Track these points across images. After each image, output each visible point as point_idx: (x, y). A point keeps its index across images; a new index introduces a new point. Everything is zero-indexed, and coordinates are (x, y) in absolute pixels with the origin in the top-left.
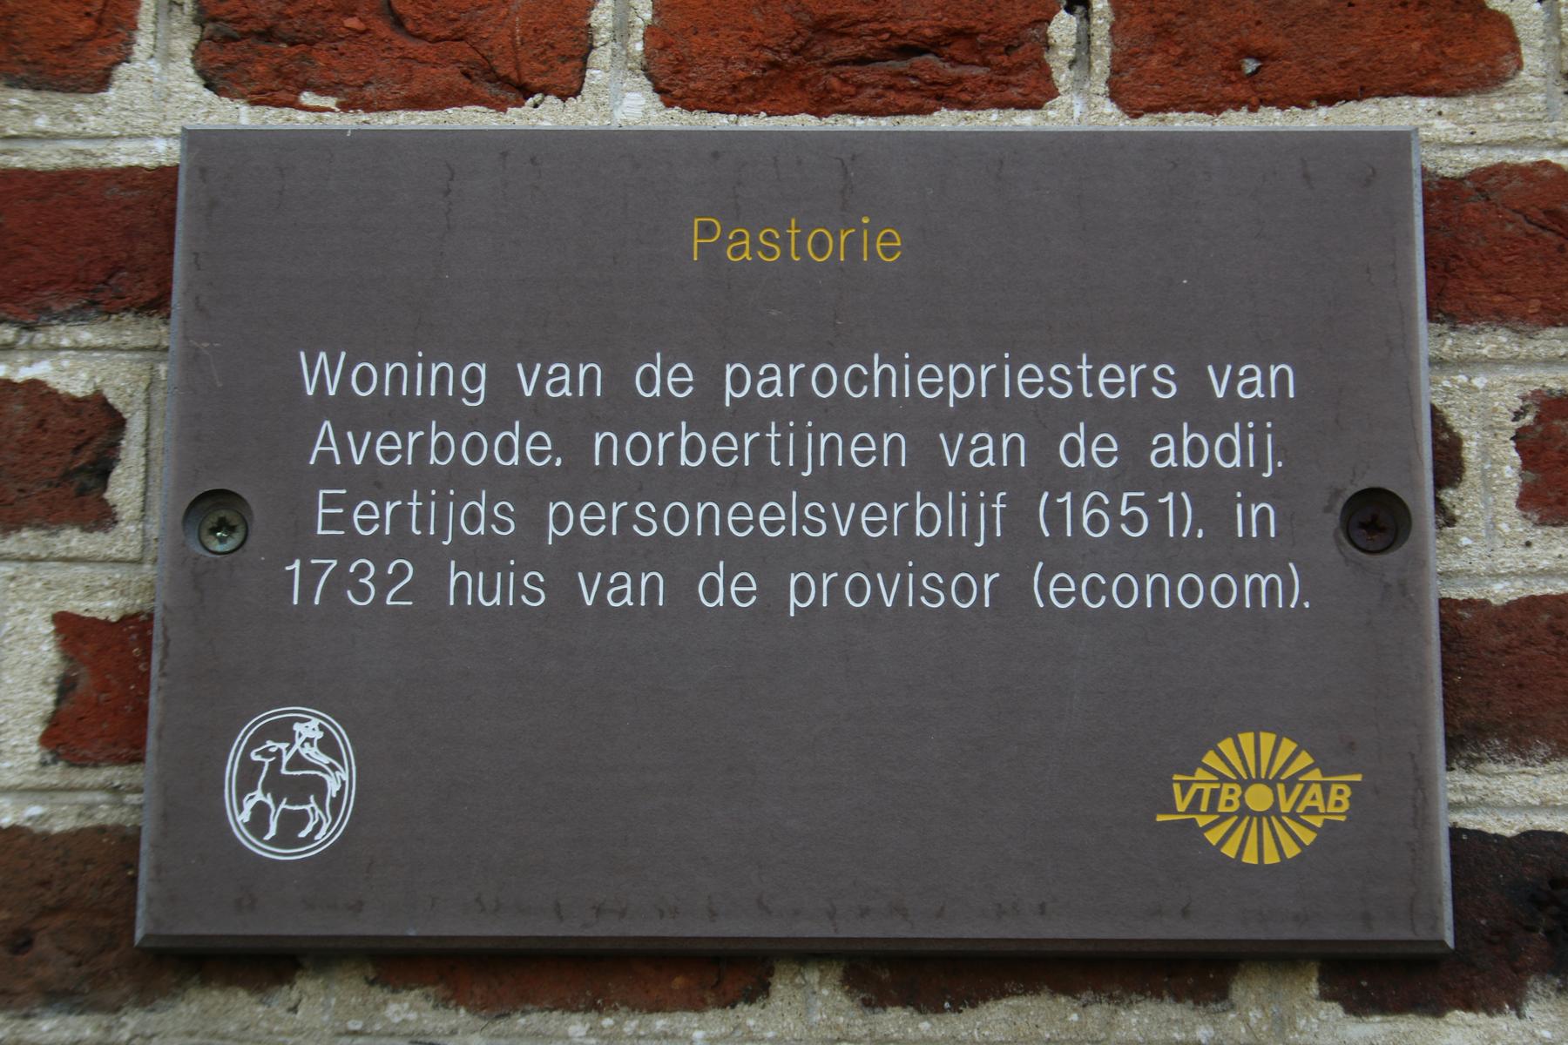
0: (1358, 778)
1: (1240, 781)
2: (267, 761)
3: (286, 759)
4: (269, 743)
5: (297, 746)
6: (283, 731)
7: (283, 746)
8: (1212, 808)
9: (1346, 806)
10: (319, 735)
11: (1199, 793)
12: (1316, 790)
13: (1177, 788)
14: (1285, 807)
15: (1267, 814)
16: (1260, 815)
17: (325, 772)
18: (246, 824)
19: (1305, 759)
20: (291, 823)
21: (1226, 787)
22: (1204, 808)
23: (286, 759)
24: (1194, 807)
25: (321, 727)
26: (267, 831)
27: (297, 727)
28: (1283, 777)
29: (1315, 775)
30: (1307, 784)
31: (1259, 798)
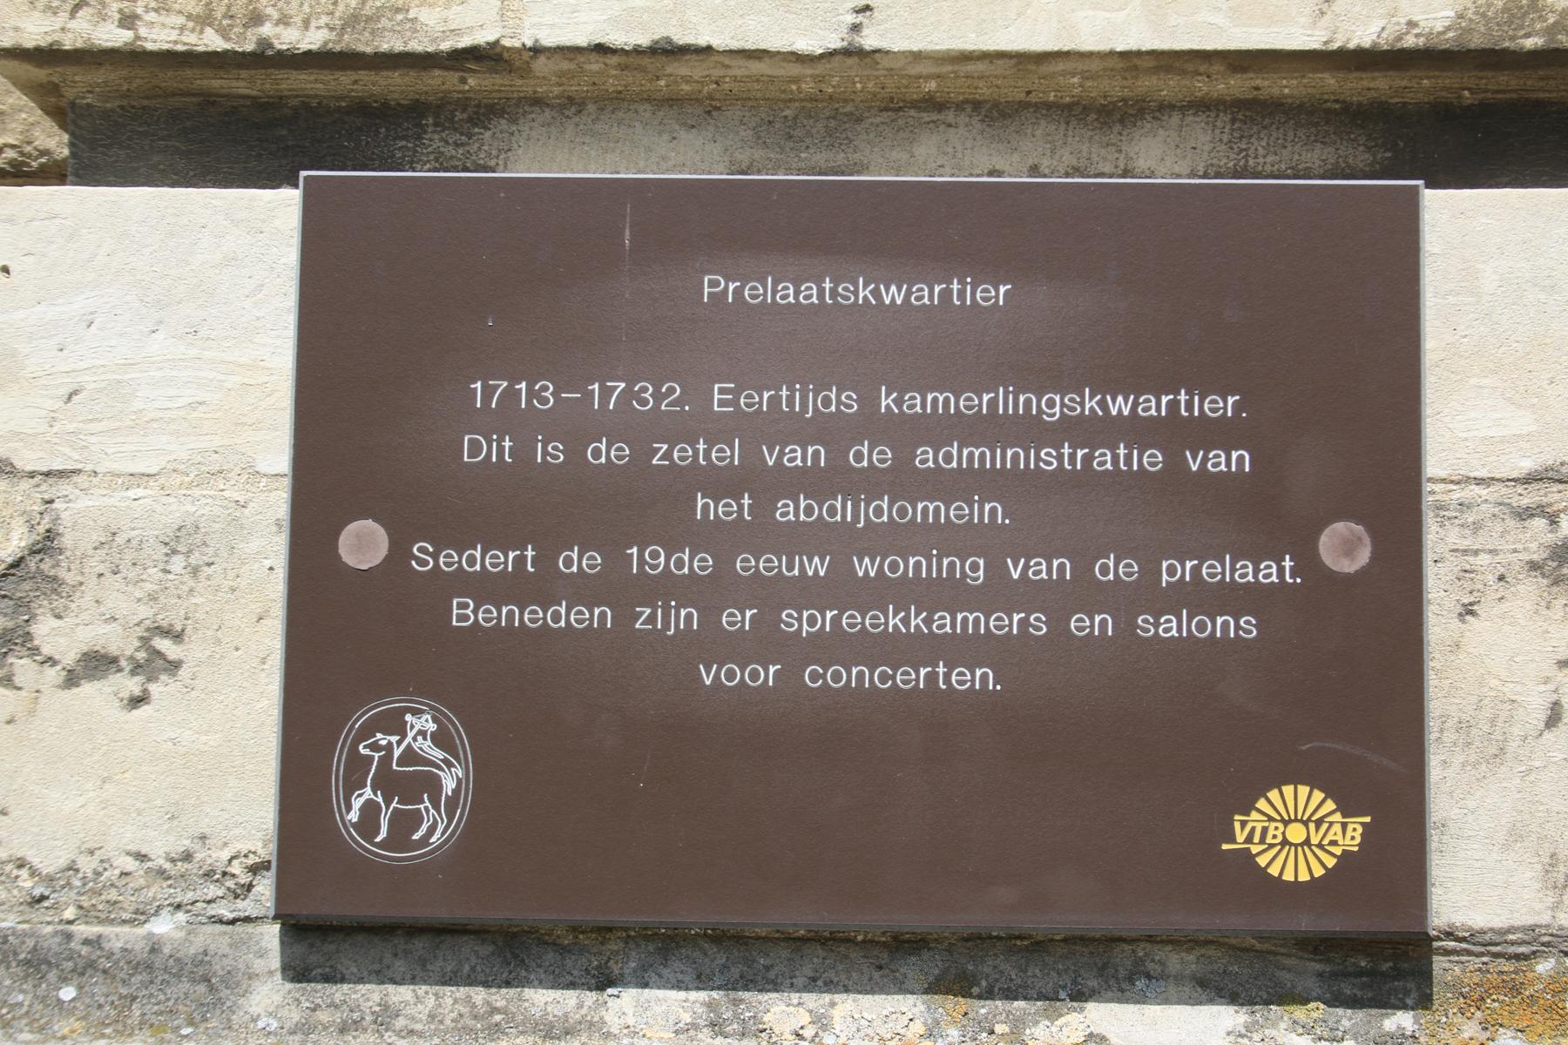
0: (1368, 819)
1: (1283, 820)
2: (377, 755)
3: (397, 753)
4: (379, 736)
5: (409, 739)
7: (394, 739)
9: (1358, 840)
11: (1253, 829)
12: (1337, 828)
13: (1237, 825)
14: (1315, 840)
15: (1302, 845)
18: (354, 825)
20: (405, 823)
21: (1273, 825)
22: (1256, 839)
23: (397, 753)
24: (1249, 840)
25: (435, 720)
27: (408, 717)
29: (1337, 817)
30: (1331, 824)
31: (1296, 833)
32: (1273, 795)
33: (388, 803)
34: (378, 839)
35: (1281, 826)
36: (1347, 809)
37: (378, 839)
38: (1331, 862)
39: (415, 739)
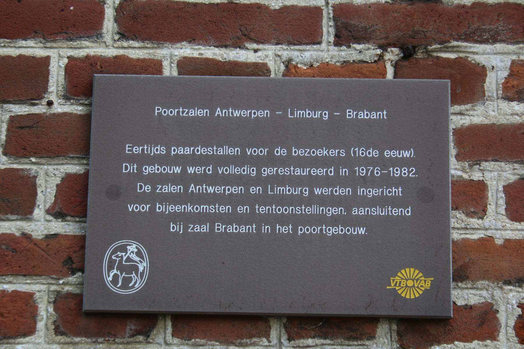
0: (432, 279)
2: (118, 259)
3: (125, 258)
4: (119, 253)
6: (123, 249)
8: (400, 285)
9: (429, 286)
10: (136, 250)
11: (397, 282)
12: (423, 282)
13: (392, 281)
14: (416, 286)
15: (412, 287)
16: (410, 287)
18: (111, 281)
19: (421, 275)
20: (127, 281)
21: (403, 281)
23: (125, 258)
24: (395, 285)
25: (137, 247)
26: (118, 284)
27: (128, 247)
29: (423, 278)
30: (421, 280)
31: (410, 283)
32: (403, 271)
33: (122, 274)
34: (118, 286)
36: (425, 276)
37: (118, 286)
38: (421, 292)
39: (130, 254)
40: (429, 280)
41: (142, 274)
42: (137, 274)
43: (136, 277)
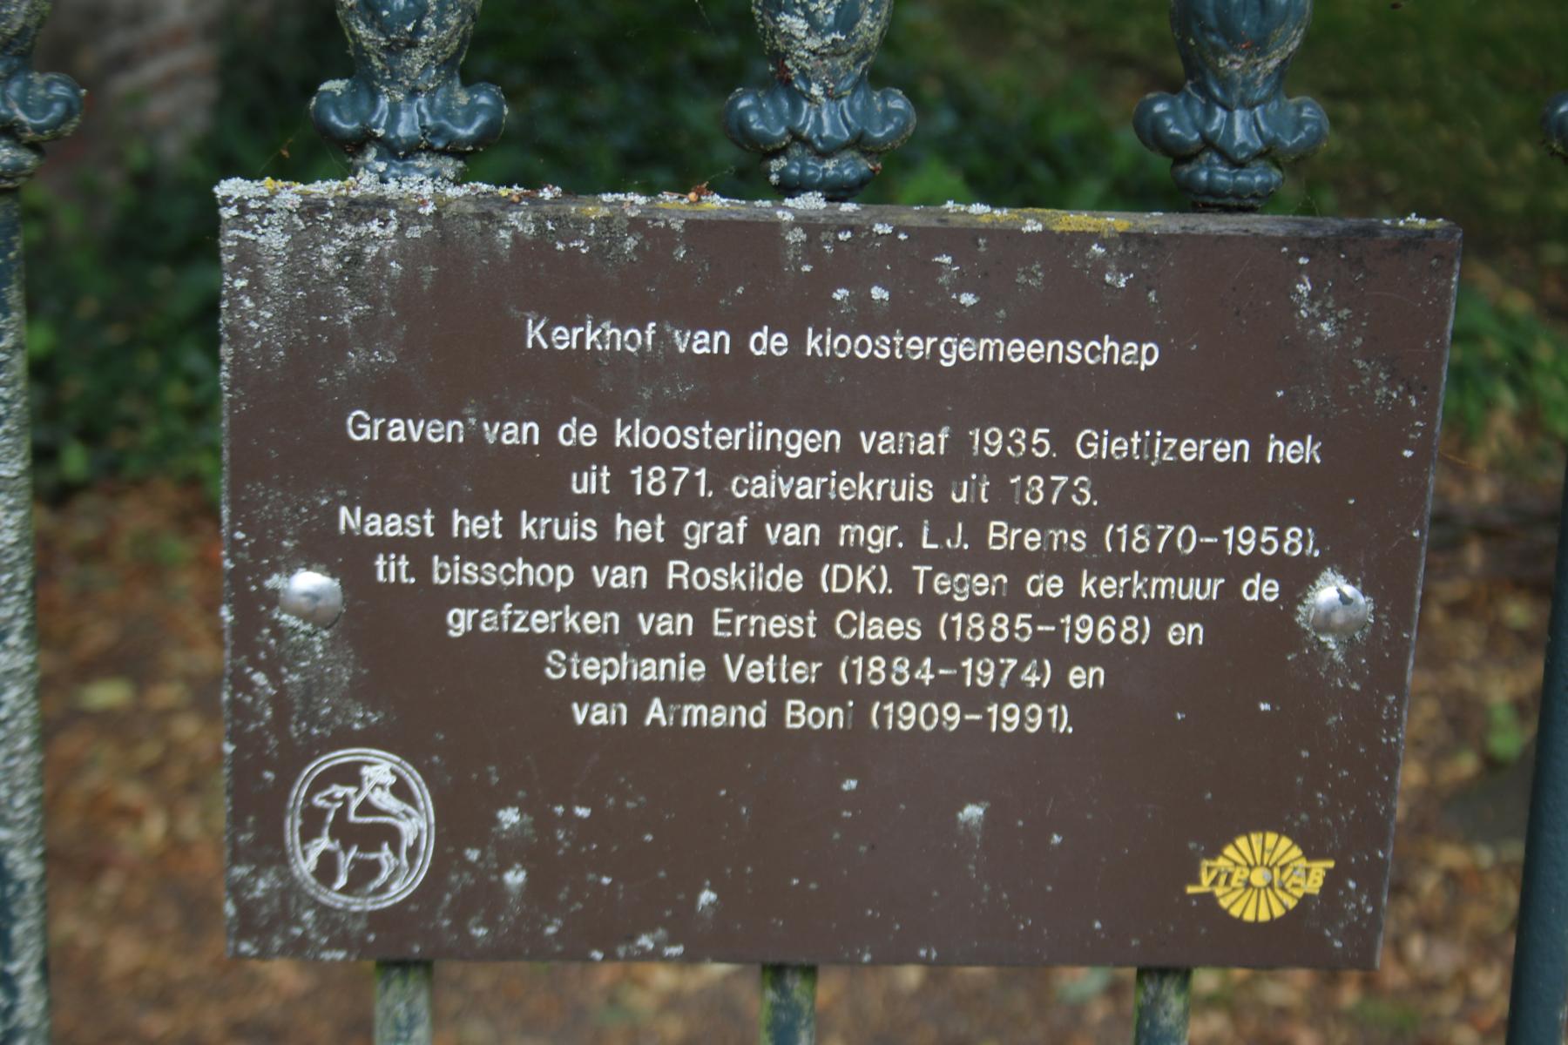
6: (350, 774)
7: (351, 790)
8: (1227, 882)
9: (1320, 882)
12: (1301, 872)
17: (396, 816)
20: (364, 872)
21: (1238, 870)
24: (1215, 882)
27: (366, 771)
28: (1281, 863)
29: (1303, 863)
31: (1259, 877)
32: (1242, 842)
35: (1246, 872)
36: (1310, 854)
38: (1292, 904)
40: (1320, 869)
41: (413, 852)
42: (395, 849)
43: (393, 860)
